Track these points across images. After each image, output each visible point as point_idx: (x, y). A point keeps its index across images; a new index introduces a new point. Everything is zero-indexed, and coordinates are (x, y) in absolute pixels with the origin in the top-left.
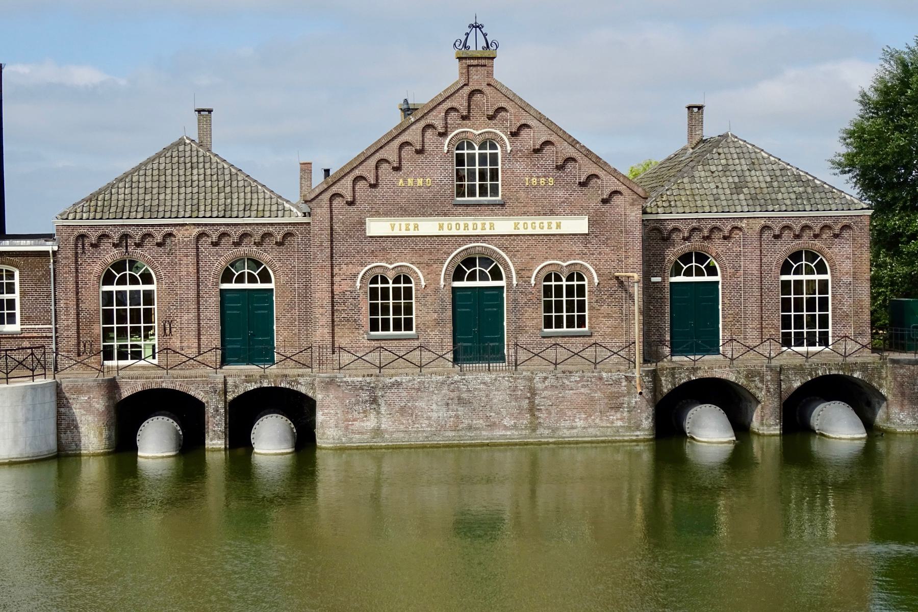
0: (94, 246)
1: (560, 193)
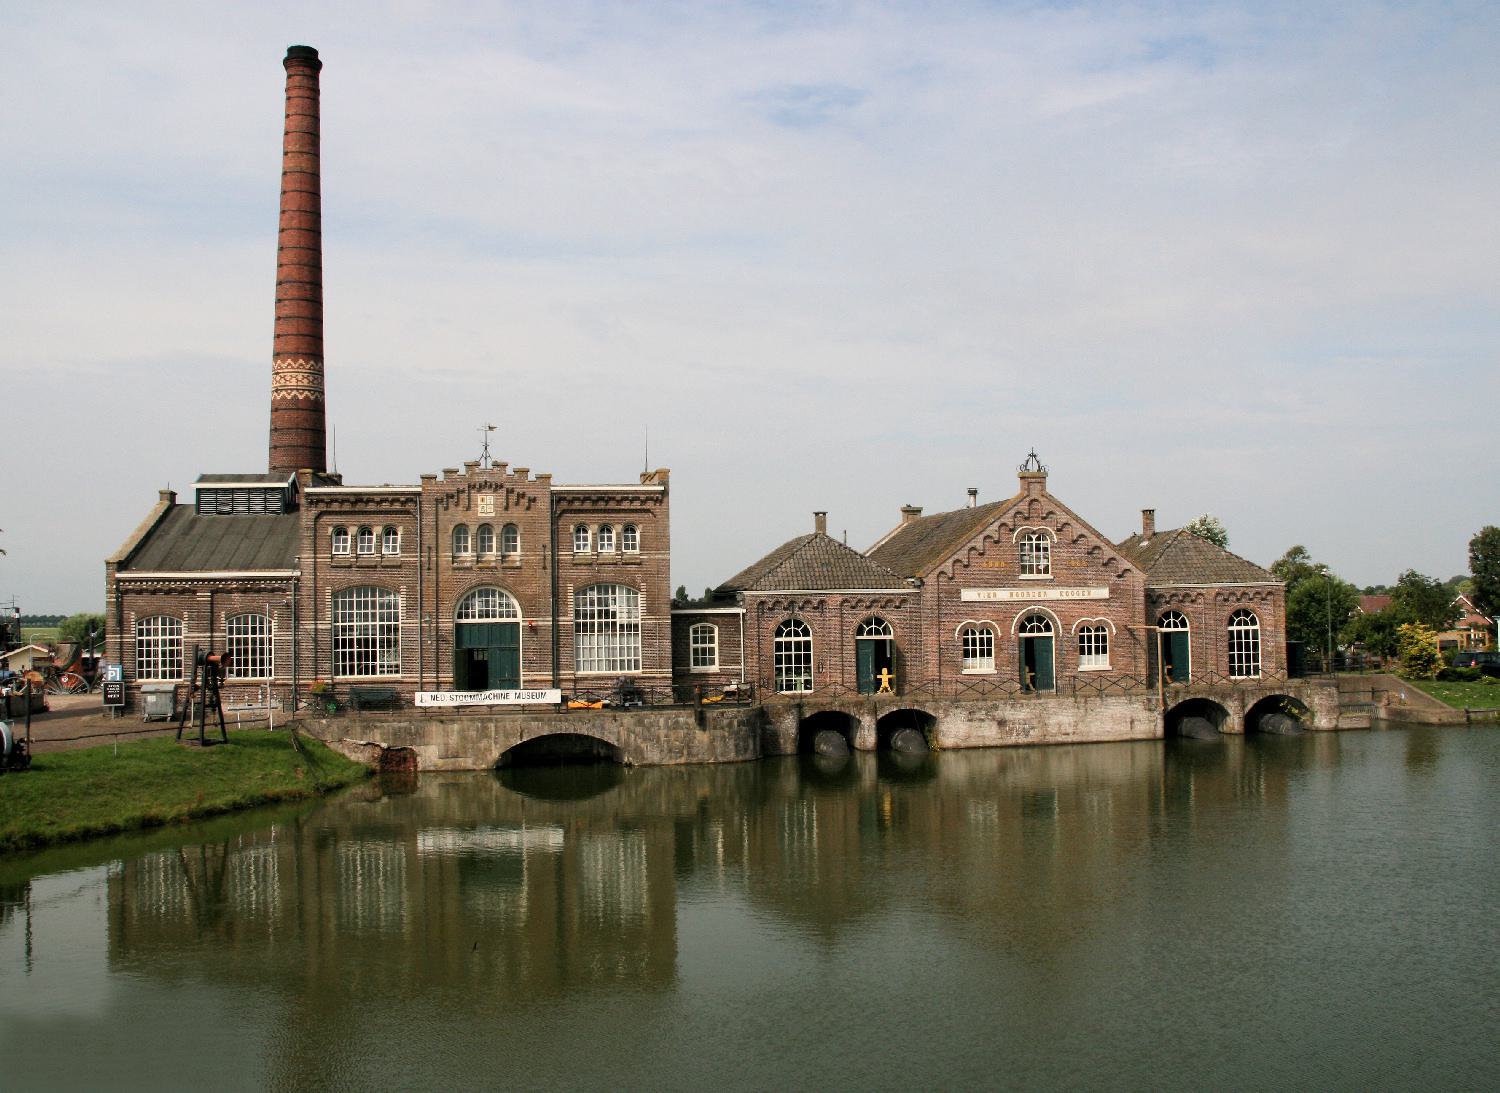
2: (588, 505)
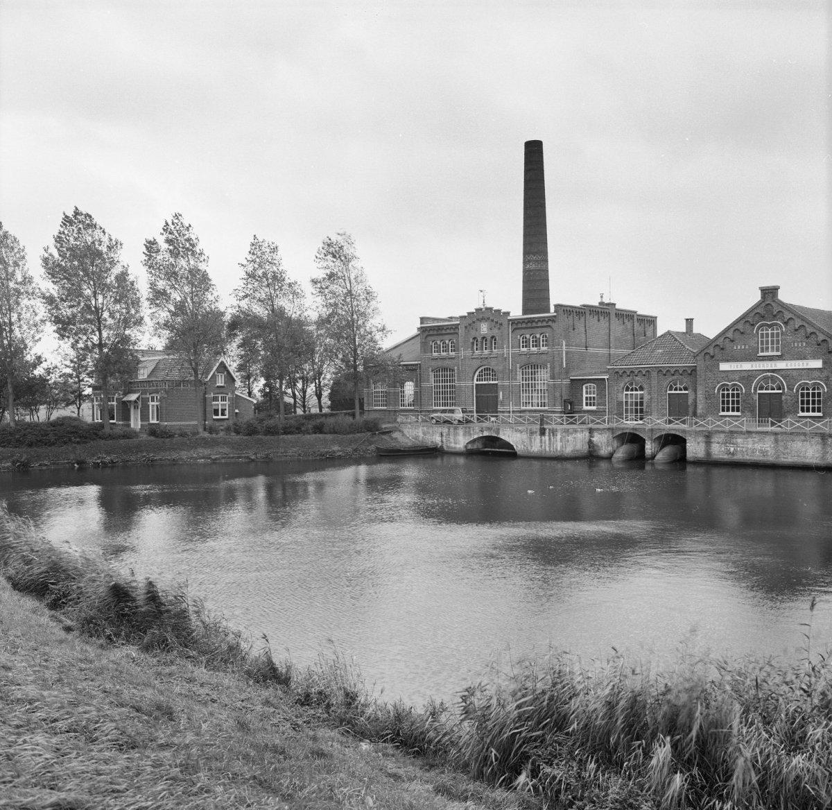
2: (524, 325)
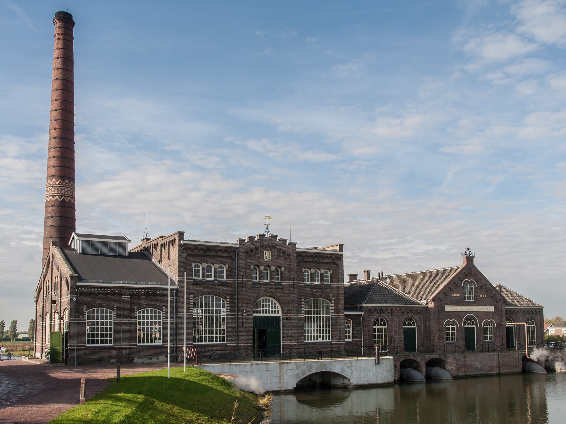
0: (372, 313)
1: (487, 299)
2: (311, 259)
